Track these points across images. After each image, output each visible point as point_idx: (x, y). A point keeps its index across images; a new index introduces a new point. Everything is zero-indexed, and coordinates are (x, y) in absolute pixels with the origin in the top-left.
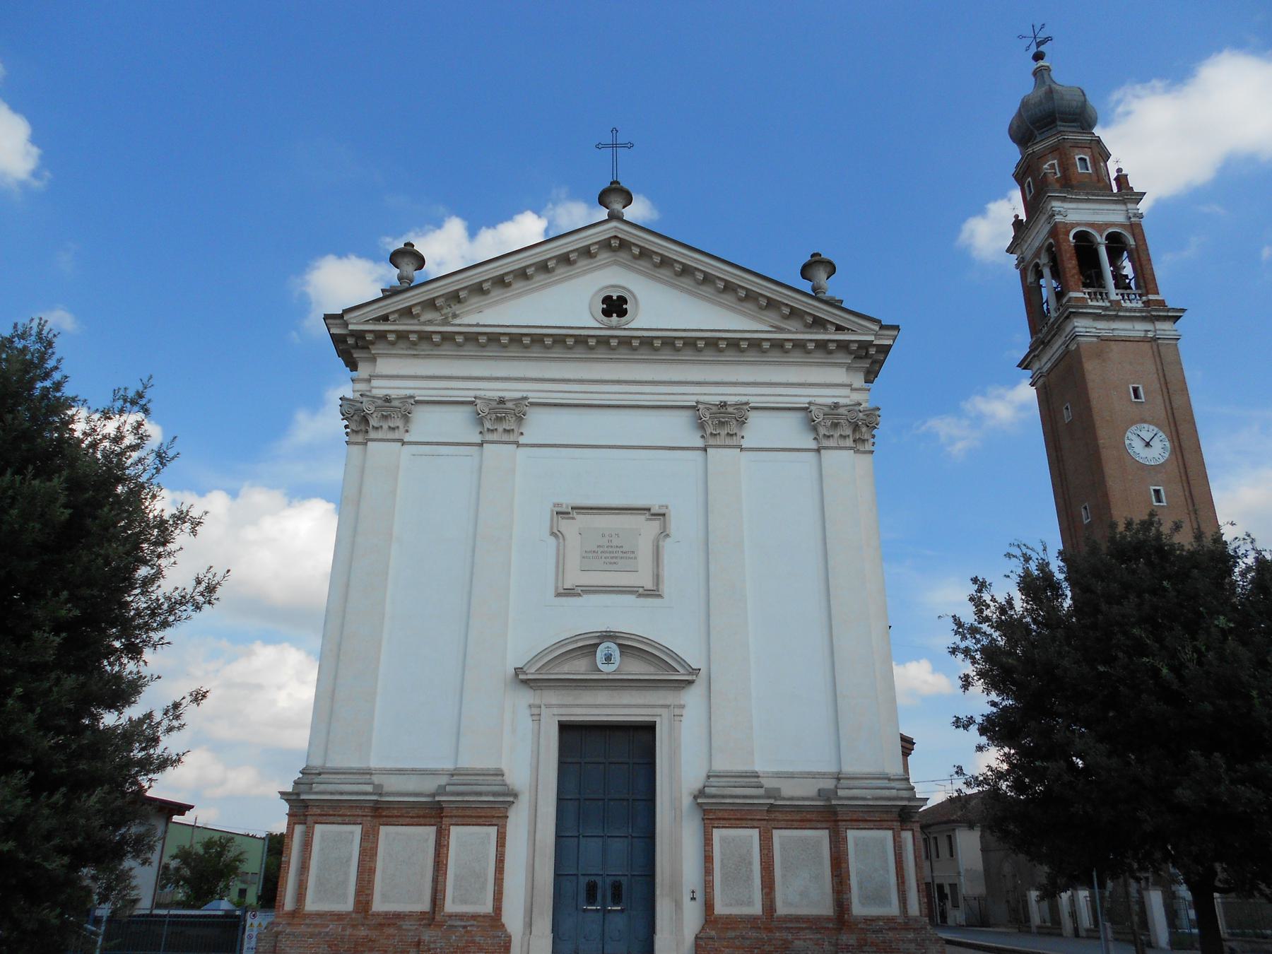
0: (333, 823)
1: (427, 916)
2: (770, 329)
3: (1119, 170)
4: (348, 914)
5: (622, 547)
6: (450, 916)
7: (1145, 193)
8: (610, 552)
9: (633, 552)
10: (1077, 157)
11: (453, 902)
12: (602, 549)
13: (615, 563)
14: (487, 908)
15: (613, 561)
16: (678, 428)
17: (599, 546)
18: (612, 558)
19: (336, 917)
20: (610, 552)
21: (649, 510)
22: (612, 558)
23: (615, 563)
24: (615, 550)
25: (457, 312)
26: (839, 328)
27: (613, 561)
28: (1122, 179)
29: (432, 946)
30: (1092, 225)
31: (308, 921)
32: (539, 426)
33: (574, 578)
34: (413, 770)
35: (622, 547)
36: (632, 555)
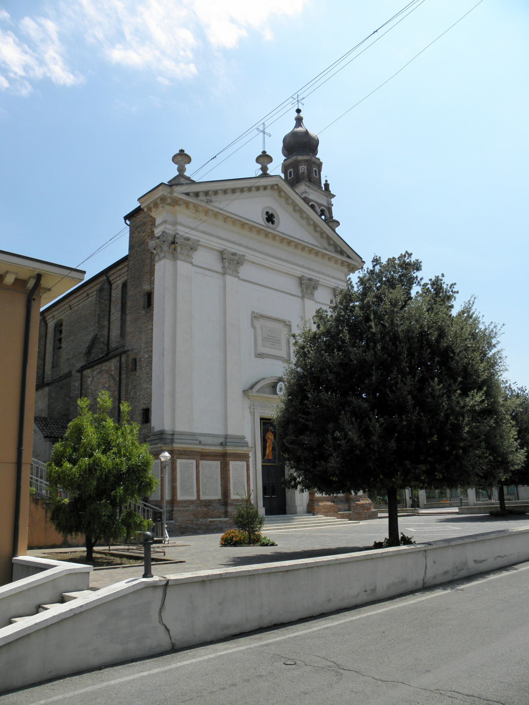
0: (184, 459)
1: (221, 501)
2: (320, 246)
3: (326, 181)
4: (195, 500)
5: (276, 337)
6: (234, 500)
7: (335, 196)
8: (273, 339)
9: (280, 341)
10: (314, 169)
11: (234, 495)
12: (269, 337)
13: (274, 345)
14: (245, 497)
15: (274, 343)
16: (293, 286)
17: (268, 336)
18: (273, 342)
19: (191, 503)
20: (273, 339)
21: (285, 322)
22: (273, 342)
23: (274, 345)
24: (273, 338)
25: (213, 200)
26: (348, 257)
27: (274, 343)
28: (327, 185)
29: (232, 513)
30: (316, 203)
31: (180, 505)
32: (245, 270)
33: (261, 350)
34: (209, 434)
35: (276, 337)
36: (280, 342)
